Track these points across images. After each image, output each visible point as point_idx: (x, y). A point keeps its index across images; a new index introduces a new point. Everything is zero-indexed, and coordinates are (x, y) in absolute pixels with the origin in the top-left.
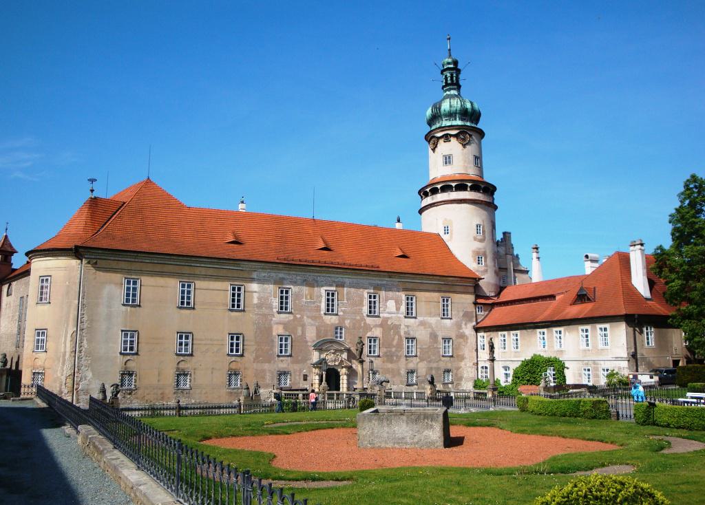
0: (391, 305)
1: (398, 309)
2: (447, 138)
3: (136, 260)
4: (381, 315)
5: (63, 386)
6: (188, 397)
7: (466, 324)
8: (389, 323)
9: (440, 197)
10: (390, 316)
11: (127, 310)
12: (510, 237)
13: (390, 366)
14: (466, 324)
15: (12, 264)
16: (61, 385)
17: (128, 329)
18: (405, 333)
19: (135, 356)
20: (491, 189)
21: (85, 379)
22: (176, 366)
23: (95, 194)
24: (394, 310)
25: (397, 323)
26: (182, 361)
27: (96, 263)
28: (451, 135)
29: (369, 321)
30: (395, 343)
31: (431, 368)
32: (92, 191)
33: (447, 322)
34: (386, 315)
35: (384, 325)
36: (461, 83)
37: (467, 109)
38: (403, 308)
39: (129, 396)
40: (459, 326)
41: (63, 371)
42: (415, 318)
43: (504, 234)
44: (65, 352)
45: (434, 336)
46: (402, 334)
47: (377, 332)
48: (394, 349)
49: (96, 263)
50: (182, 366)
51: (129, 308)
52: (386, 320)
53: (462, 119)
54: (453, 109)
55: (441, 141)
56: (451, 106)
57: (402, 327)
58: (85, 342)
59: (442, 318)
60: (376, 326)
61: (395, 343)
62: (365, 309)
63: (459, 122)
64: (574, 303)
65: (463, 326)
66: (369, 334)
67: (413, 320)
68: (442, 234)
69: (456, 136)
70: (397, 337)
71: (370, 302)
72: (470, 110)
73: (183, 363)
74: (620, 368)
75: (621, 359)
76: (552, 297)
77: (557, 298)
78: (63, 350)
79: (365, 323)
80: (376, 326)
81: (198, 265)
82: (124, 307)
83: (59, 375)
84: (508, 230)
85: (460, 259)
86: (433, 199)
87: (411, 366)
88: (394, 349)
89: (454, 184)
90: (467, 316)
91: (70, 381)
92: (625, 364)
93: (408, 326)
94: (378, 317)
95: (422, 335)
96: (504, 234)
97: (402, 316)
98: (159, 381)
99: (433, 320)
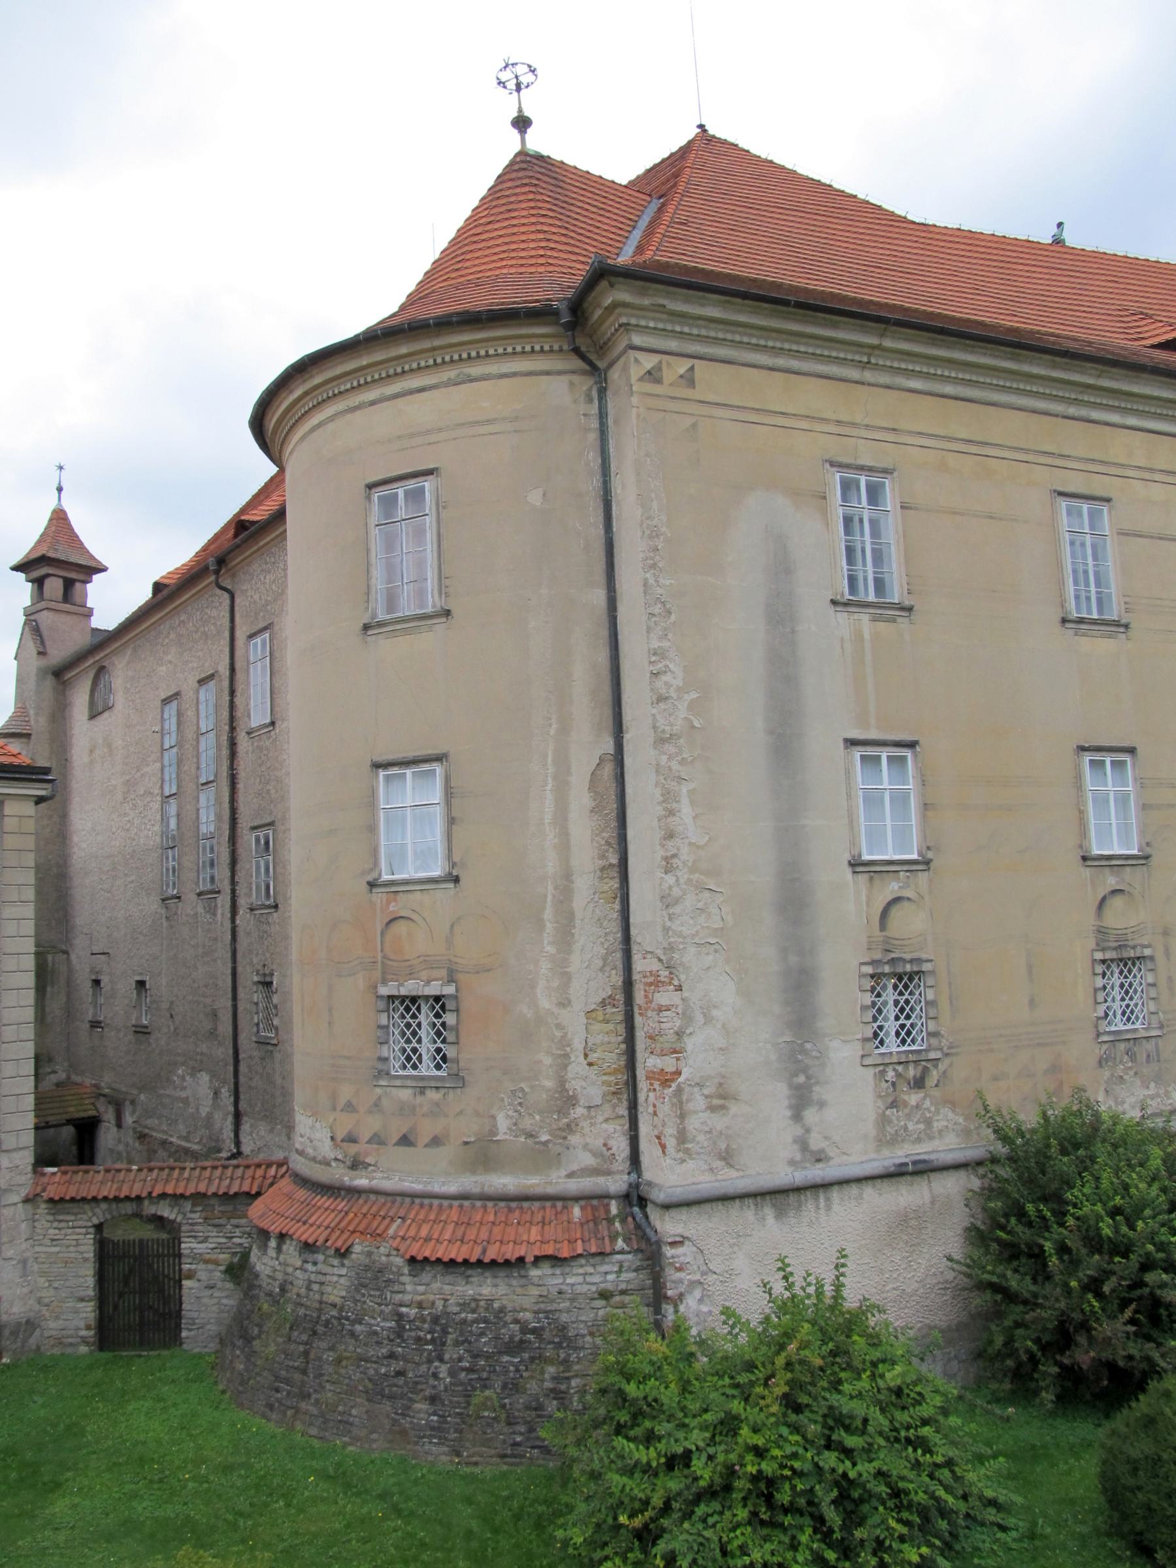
3: (868, 376)
5: (578, 1066)
6: (1158, 1079)
11: (858, 637)
15: (89, 613)
16: (564, 1061)
17: (873, 735)
19: (923, 878)
21: (708, 1020)
22: (1090, 920)
23: (538, 141)
26: (1115, 892)
27: (689, 379)
32: (522, 123)
39: (913, 1098)
41: (566, 978)
44: (568, 875)
49: (689, 379)
50: (1118, 917)
51: (864, 618)
58: (686, 810)
73: (1118, 902)
78: (552, 866)
81: (1115, 418)
82: (842, 620)
83: (545, 1003)
91: (608, 1036)
98: (1032, 1003)
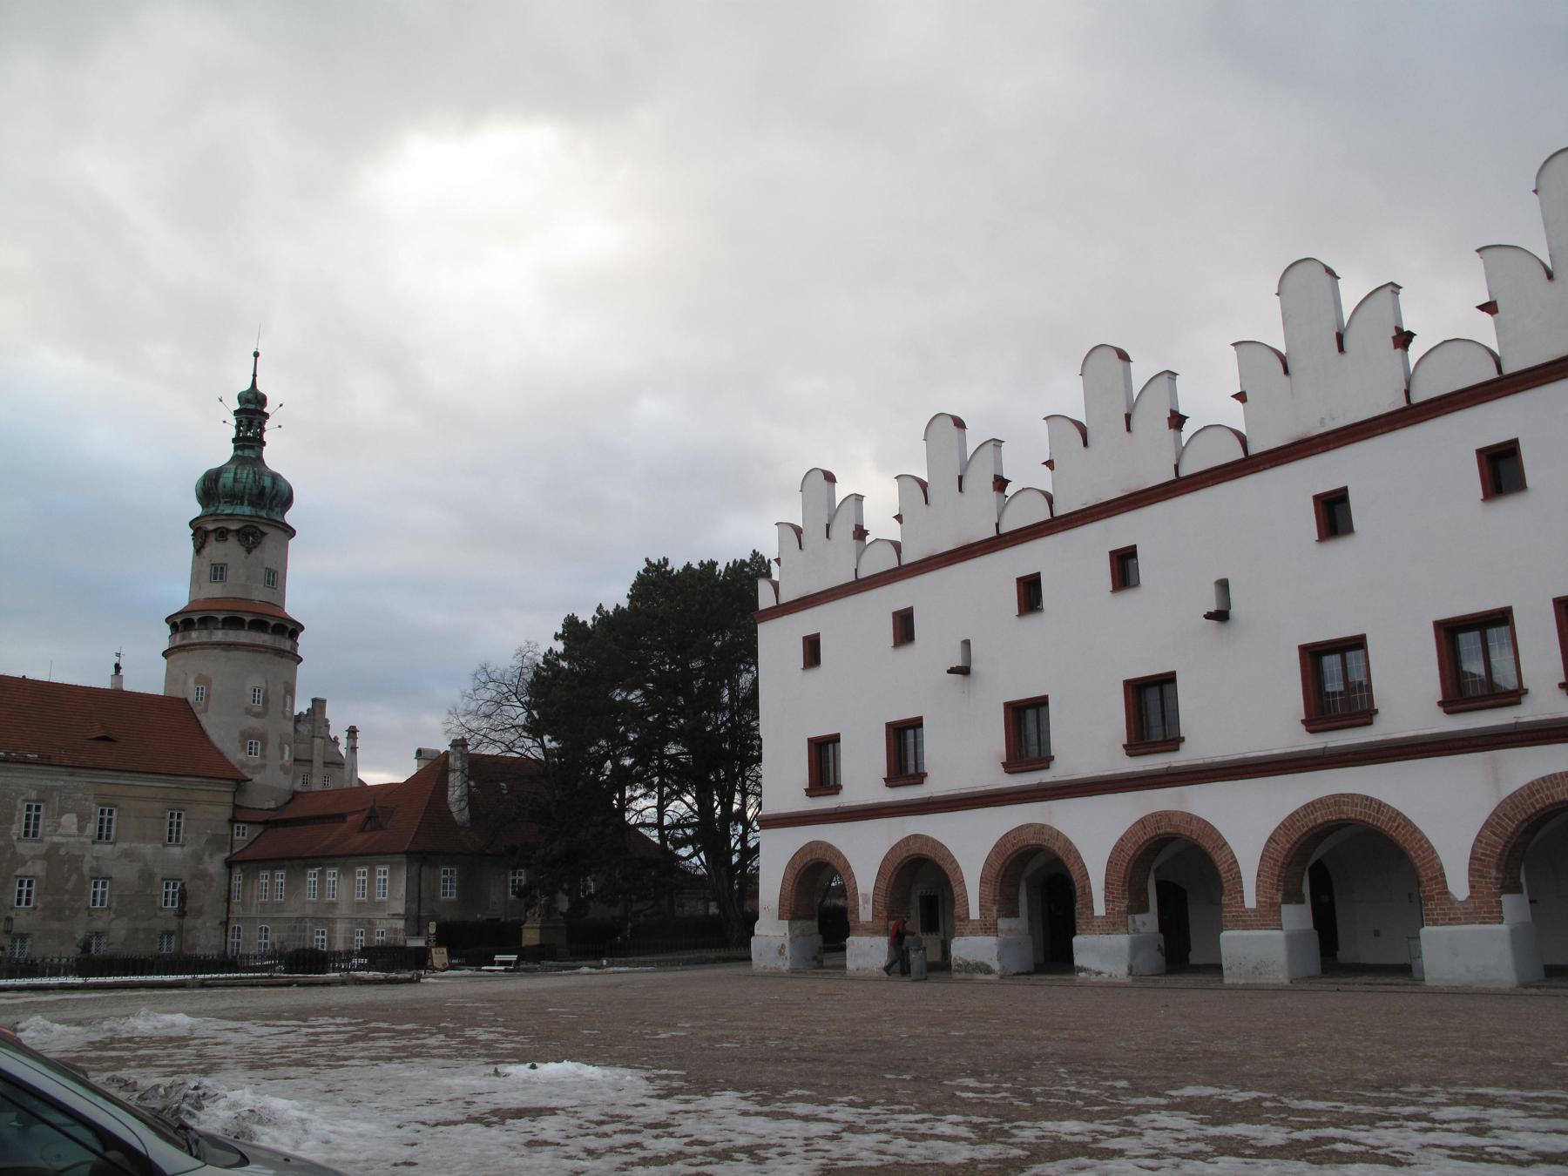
0: (70, 821)
1: (81, 829)
2: (222, 534)
4: (47, 839)
7: (211, 856)
8: (62, 852)
9: (195, 636)
10: (64, 840)
12: (323, 708)
13: (56, 925)
14: (211, 856)
18: (91, 869)
20: (290, 627)
24: (74, 830)
25: (77, 853)
28: (228, 531)
29: (24, 848)
30: (70, 886)
31: (137, 930)
33: (176, 851)
34: (55, 839)
35: (51, 855)
36: (266, 437)
37: (264, 488)
38: (92, 828)
40: (197, 858)
42: (113, 843)
43: (314, 701)
45: (147, 877)
46: (86, 869)
47: (37, 868)
48: (66, 897)
52: (55, 847)
53: (251, 504)
54: (239, 486)
55: (212, 539)
56: (235, 480)
57: (88, 858)
59: (165, 845)
60: (35, 857)
61: (70, 886)
62: (17, 829)
63: (247, 510)
64: (362, 829)
65: (206, 858)
66: (19, 872)
67: (109, 847)
68: (192, 699)
69: (237, 532)
70: (74, 877)
71: (28, 817)
72: (268, 490)
74: (396, 931)
75: (395, 916)
76: (341, 817)
77: (349, 819)
79: (14, 853)
80: (35, 857)
84: (320, 696)
85: (218, 744)
86: (183, 638)
87: (98, 925)
88: (66, 897)
89: (220, 617)
90: (215, 842)
92: (400, 924)
93: (97, 859)
94: (41, 841)
95: (125, 873)
96: (314, 701)
97: (88, 840)
99: (148, 849)
